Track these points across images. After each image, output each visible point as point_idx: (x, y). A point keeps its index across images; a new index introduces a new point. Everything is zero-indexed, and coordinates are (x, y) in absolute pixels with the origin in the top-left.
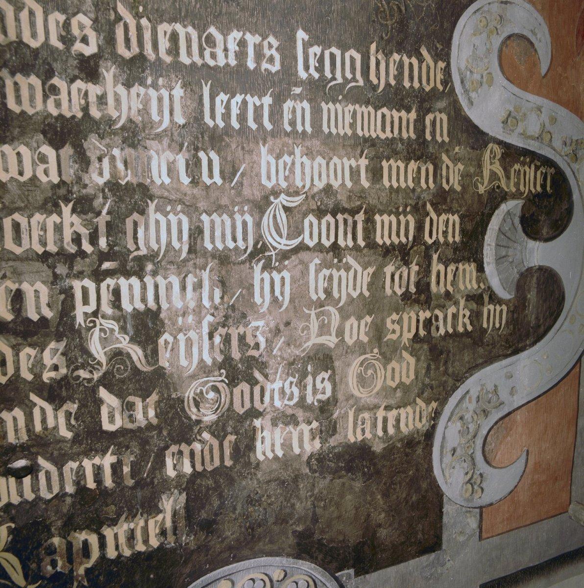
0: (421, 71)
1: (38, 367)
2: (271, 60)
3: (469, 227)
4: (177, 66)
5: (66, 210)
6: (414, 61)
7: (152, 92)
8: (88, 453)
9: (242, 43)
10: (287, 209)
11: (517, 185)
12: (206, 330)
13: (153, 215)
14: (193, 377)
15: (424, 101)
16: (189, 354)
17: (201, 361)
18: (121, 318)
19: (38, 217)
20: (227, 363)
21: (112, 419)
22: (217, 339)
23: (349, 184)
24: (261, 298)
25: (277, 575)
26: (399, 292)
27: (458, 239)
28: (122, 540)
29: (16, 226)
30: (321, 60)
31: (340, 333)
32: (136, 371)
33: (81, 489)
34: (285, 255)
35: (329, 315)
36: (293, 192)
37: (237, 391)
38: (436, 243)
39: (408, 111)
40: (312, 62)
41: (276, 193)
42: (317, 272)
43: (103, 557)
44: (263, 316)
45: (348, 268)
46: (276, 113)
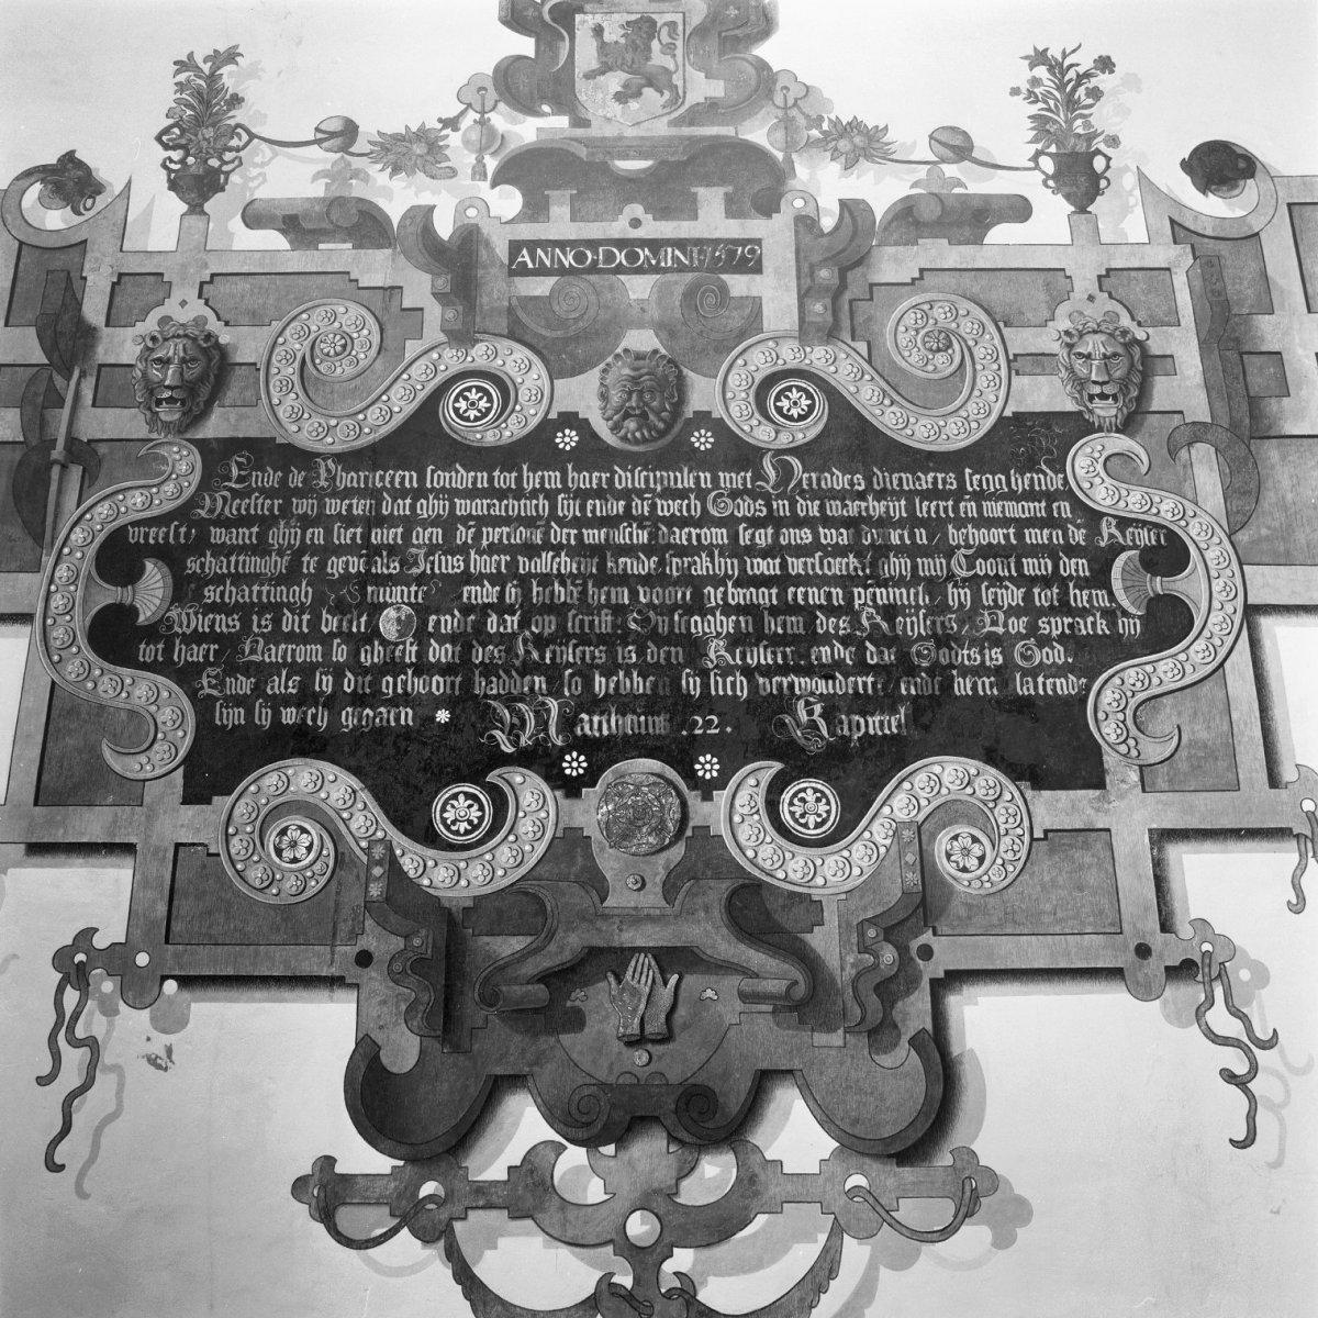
0: (1050, 480)
1: (837, 627)
2: (951, 484)
3: (1096, 567)
4: (902, 491)
5: (851, 556)
6: (1042, 476)
7: (891, 504)
8: (860, 674)
9: (935, 478)
10: (965, 556)
11: (1133, 540)
12: (921, 617)
13: (892, 559)
14: (916, 640)
15: (1050, 497)
16: (912, 630)
17: (919, 633)
18: (876, 606)
19: (839, 559)
20: (935, 635)
21: (872, 659)
22: (928, 623)
23: (1003, 542)
24: (953, 602)
25: (973, 771)
26: (1046, 605)
27: (1087, 574)
28: (877, 725)
29: (829, 563)
30: (981, 481)
31: (1005, 625)
32: (884, 635)
33: (856, 692)
34: (964, 580)
35: (997, 615)
36: (968, 546)
37: (941, 652)
38: (1070, 575)
39: (1040, 502)
40: (975, 483)
41: (958, 547)
42: (987, 588)
43: (867, 732)
44: (953, 612)
45: (1007, 588)
46: (956, 509)
